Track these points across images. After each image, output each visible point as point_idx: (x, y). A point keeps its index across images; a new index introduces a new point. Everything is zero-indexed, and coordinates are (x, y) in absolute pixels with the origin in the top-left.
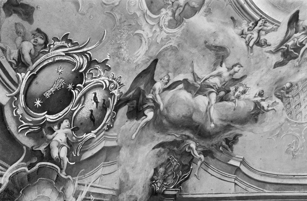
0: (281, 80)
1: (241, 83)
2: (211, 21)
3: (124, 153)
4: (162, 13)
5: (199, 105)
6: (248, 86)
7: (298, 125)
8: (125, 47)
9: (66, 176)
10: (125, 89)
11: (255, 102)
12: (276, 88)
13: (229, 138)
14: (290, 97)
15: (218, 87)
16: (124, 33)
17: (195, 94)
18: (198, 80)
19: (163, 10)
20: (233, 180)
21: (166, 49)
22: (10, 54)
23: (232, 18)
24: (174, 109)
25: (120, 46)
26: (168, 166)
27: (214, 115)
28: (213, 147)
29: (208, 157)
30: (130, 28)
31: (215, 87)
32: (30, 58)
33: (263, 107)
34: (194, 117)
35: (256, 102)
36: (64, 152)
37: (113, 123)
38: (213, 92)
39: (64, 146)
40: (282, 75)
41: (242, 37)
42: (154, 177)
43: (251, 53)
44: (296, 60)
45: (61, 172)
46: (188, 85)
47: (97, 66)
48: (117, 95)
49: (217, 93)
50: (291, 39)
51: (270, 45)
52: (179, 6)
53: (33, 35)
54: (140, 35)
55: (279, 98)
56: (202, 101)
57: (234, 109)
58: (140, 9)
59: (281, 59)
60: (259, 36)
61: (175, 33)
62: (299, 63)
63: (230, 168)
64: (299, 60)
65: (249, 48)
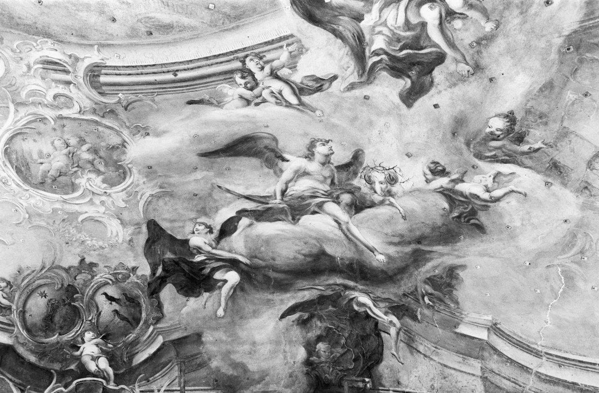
0: (459, 123)
1: (364, 166)
2: (164, 132)
5: (321, 231)
9: (118, 386)
11: (438, 190)
13: (434, 276)
17: (290, 218)
18: (268, 199)
21: (148, 203)
23: (190, 103)
31: (318, 194)
34: (329, 250)
35: (444, 190)
36: (103, 363)
38: (324, 202)
39: (100, 357)
42: (311, 359)
44: (448, 61)
46: (264, 214)
49: (337, 201)
50: (367, 37)
51: (335, 78)
52: (92, 163)
54: (91, 219)
57: (404, 218)
58: (53, 202)
61: (132, 183)
62: (467, 64)
64: (459, 57)
65: (298, 107)
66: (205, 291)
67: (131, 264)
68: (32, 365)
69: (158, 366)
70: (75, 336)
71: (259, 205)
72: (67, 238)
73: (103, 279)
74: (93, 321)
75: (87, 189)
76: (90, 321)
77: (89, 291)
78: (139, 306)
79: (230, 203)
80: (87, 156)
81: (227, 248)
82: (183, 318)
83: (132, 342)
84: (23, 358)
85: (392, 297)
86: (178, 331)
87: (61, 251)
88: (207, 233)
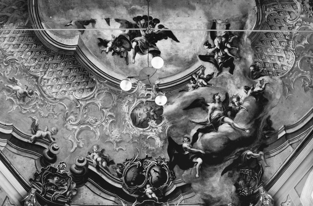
0: (244, 72)
2: (174, 102)
3: (195, 186)
4: (150, 124)
6: (235, 95)
7: (293, 71)
10: (168, 159)
12: (249, 77)
14: (263, 69)
15: (223, 113)
17: (215, 129)
19: (148, 123)
20: (288, 144)
21: (169, 130)
22: (115, 175)
23: (180, 91)
24: (212, 147)
26: (244, 177)
27: (240, 126)
28: (262, 141)
29: (265, 149)
31: (221, 116)
33: (259, 91)
34: (231, 138)
36: (154, 195)
37: (175, 176)
38: (223, 118)
40: (241, 70)
41: (197, 88)
43: (212, 85)
44: (235, 59)
46: (206, 130)
47: (145, 160)
48: (166, 164)
49: (227, 116)
50: (217, 60)
51: (214, 73)
52: (153, 116)
54: (151, 138)
55: (259, 77)
56: (224, 128)
57: (247, 111)
59: (228, 68)
60: (203, 78)
63: (281, 140)
67: (163, 157)
79: (194, 127)
80: (152, 114)
85: (257, 145)
88: (188, 141)
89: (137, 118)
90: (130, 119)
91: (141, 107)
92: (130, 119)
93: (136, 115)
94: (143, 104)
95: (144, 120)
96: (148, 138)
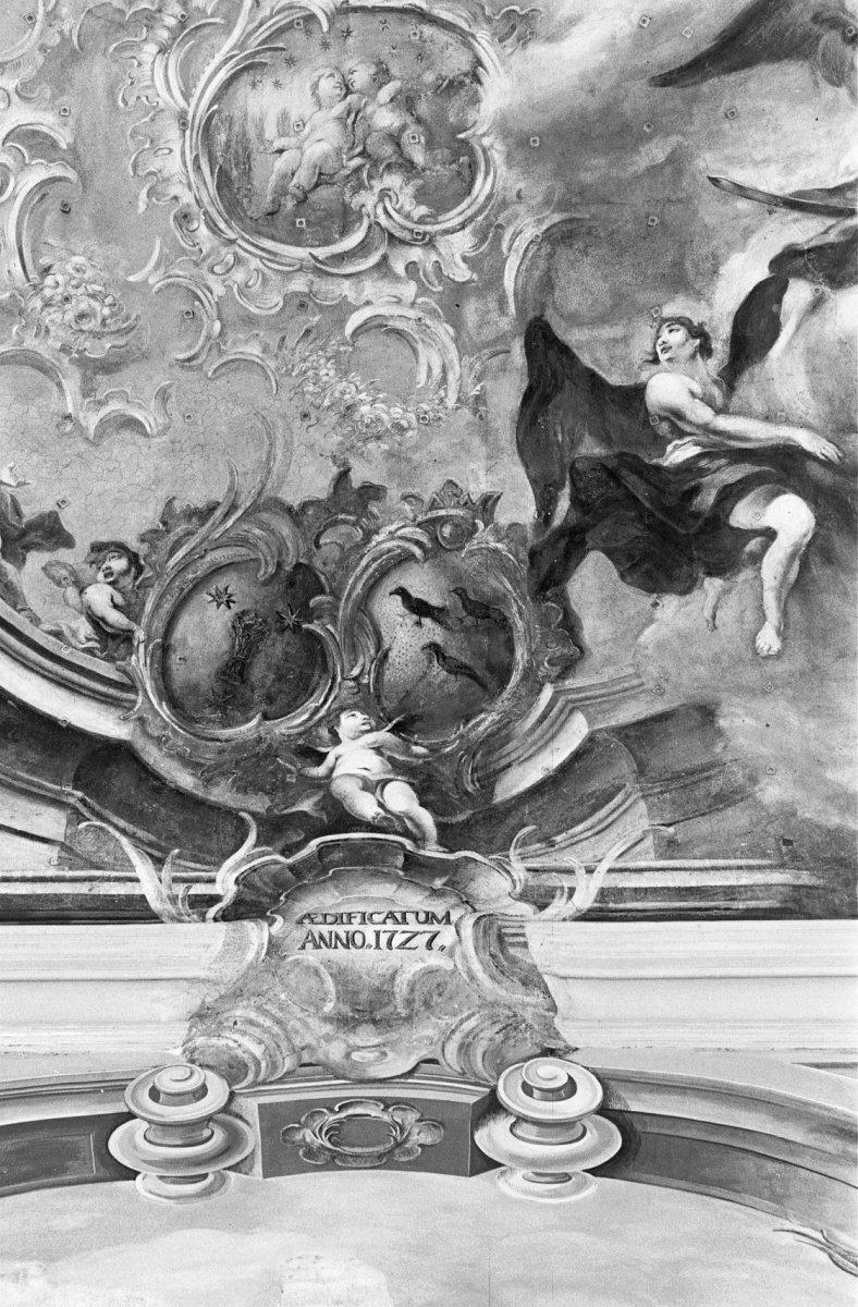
4: (369, 208)
8: (363, 396)
16: (317, 369)
22: (74, 634)
25: (342, 408)
30: (315, 339)
32: (123, 616)
36: (400, 797)
39: (391, 780)
45: (418, 847)
52: (395, 138)
53: (94, 565)
54: (376, 326)
58: (288, 273)
61: (489, 197)
66: (709, 574)
67: (477, 488)
68: (180, 794)
69: (581, 802)
70: (311, 723)
71: (830, 222)
72: (308, 396)
73: (395, 543)
74: (365, 681)
75: (378, 224)
76: (355, 679)
77: (354, 585)
78: (504, 627)
79: (747, 233)
80: (386, 118)
81: (759, 407)
82: (646, 656)
83: (489, 736)
84: (158, 777)
86: (634, 697)
87: (288, 445)
88: (693, 357)
89: (258, 160)
90: (198, 168)
91: (291, 62)
92: (198, 168)
93: (252, 133)
94: (308, 32)
95: (322, 179)
96: (349, 328)
